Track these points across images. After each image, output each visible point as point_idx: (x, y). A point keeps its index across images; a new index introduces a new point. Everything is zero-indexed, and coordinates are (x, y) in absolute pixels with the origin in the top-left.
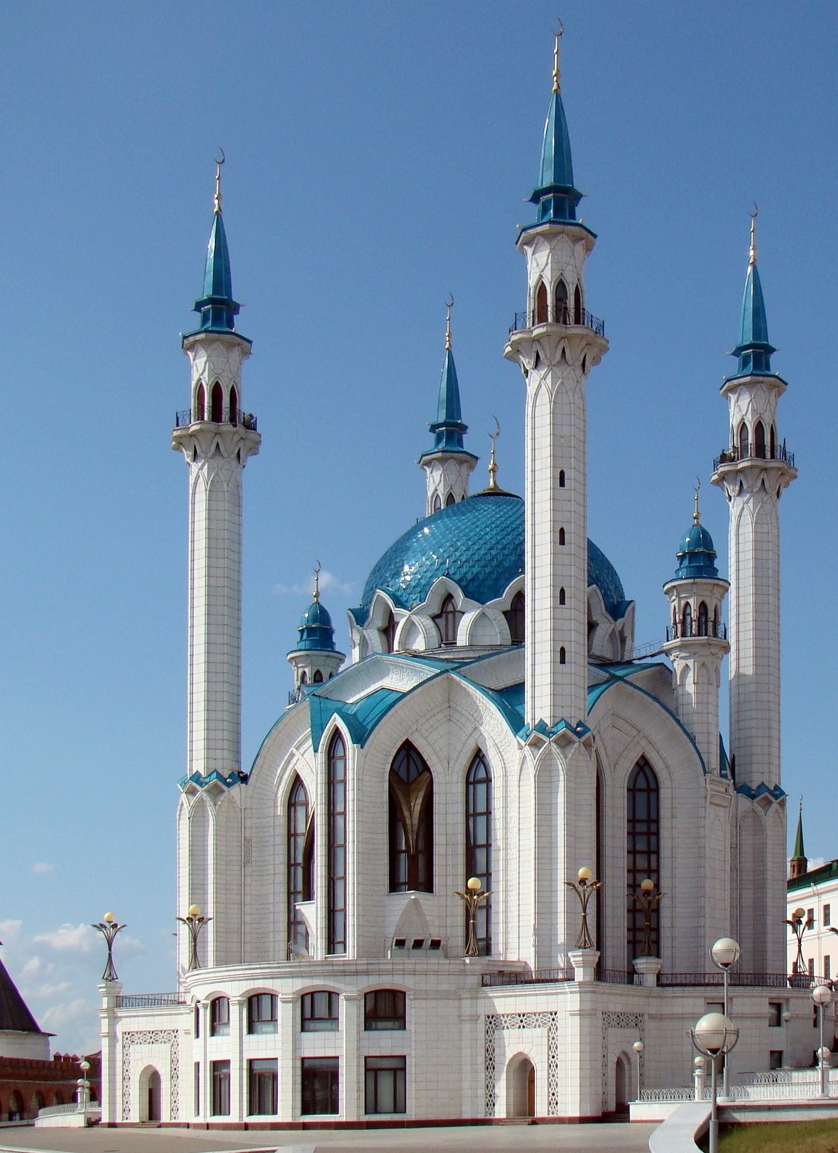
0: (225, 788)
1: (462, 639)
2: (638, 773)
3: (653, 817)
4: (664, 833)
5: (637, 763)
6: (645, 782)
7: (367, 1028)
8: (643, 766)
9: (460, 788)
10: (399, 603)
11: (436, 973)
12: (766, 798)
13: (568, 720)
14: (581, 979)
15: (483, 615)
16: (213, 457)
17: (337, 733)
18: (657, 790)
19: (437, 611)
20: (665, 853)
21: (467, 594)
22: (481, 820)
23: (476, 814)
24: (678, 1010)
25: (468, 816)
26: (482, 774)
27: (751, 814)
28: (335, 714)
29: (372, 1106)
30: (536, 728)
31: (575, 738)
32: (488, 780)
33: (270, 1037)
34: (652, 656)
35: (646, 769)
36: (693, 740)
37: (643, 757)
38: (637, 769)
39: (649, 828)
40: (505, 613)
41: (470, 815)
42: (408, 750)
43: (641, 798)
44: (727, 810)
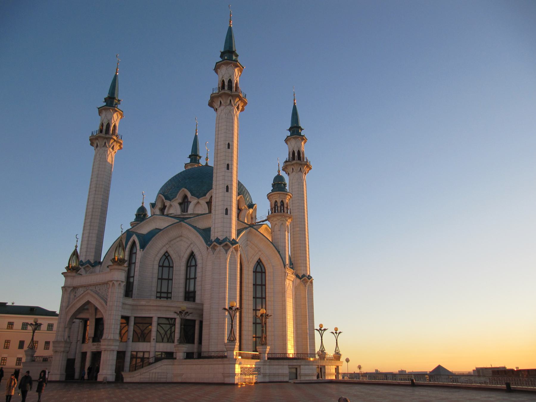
1: (190, 211)
3: (264, 283)
5: (257, 261)
6: (260, 269)
8: (259, 262)
9: (183, 268)
10: (167, 198)
12: (304, 279)
15: (198, 203)
16: (103, 146)
17: (134, 243)
18: (265, 273)
19: (180, 201)
21: (193, 194)
22: (192, 281)
23: (190, 279)
25: (186, 279)
26: (193, 263)
28: (134, 236)
30: (215, 241)
32: (196, 266)
34: (263, 221)
35: (261, 263)
36: (279, 252)
37: (259, 259)
40: (207, 203)
41: (187, 279)
43: (259, 275)
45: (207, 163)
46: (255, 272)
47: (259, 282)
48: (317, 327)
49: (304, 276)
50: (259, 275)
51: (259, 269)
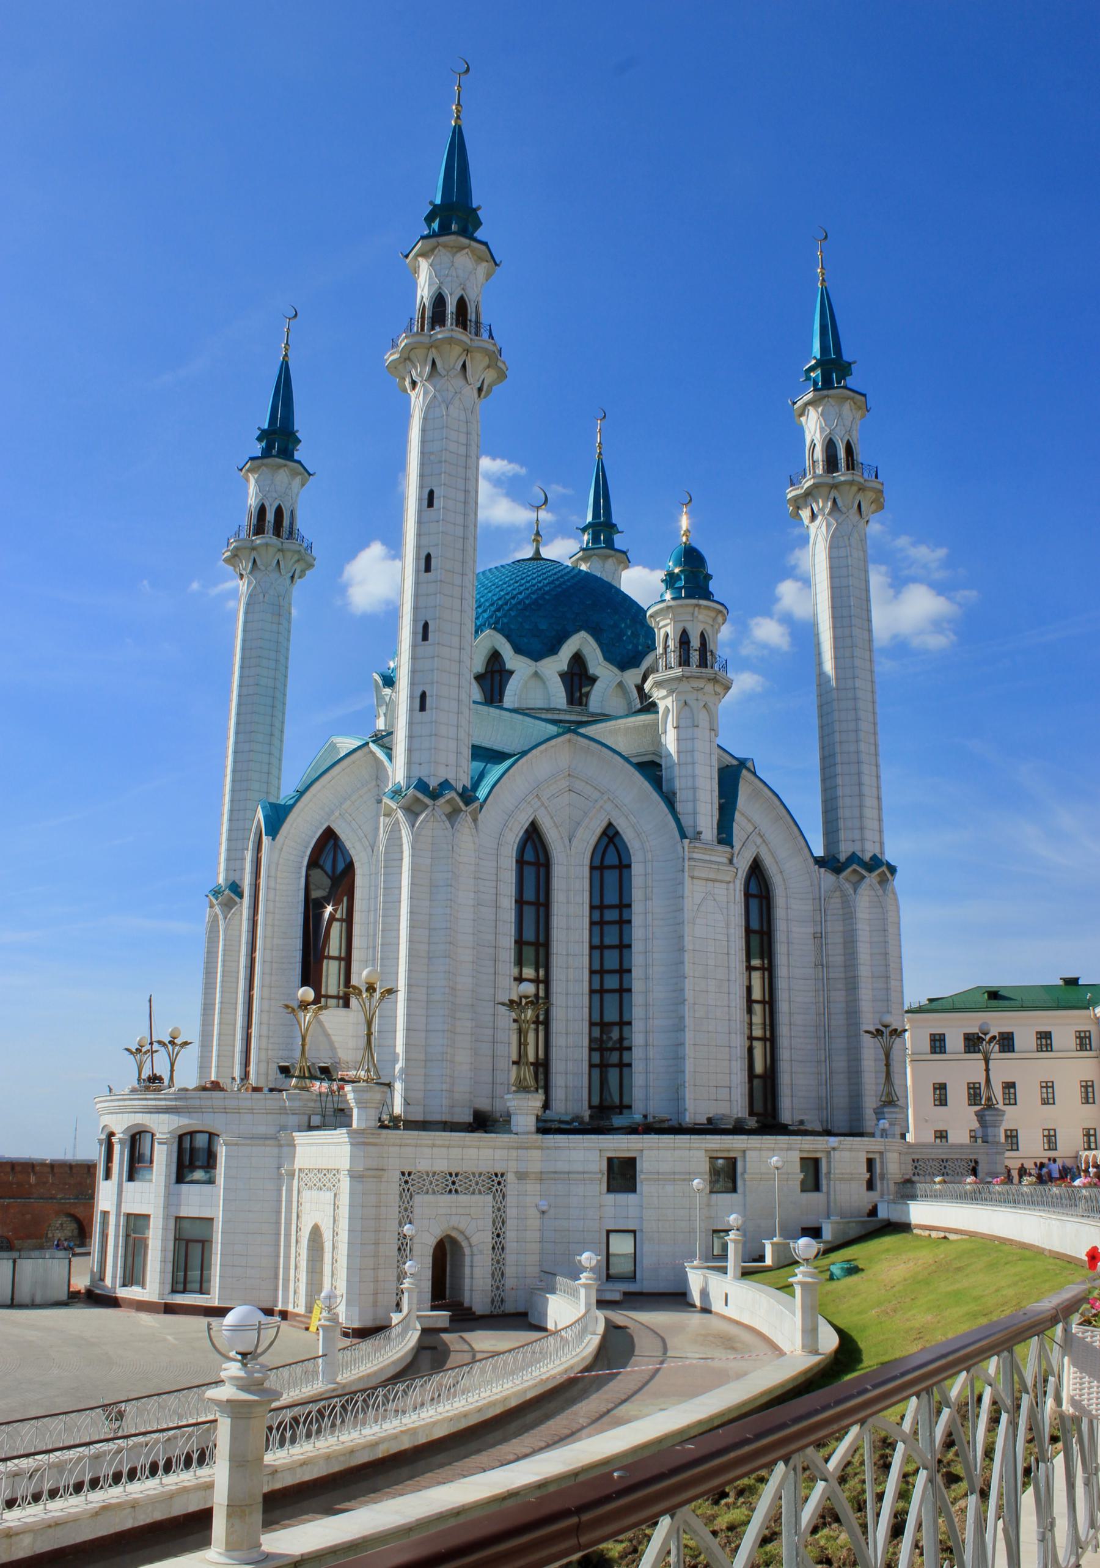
0: (237, 899)
2: (607, 847)
4: (637, 920)
5: (604, 833)
7: (180, 1179)
8: (610, 837)
11: (251, 1110)
13: (425, 779)
14: (363, 1126)
18: (629, 866)
20: (637, 947)
24: (561, 1166)
27: (838, 894)
29: (180, 1285)
31: (427, 800)
33: (146, 1185)
36: (670, 800)
37: (610, 825)
38: (605, 840)
39: (602, 916)
42: (329, 839)
43: (611, 877)
44: (731, 885)
45: (537, 552)
46: (598, 868)
47: (611, 898)
48: (869, 1022)
49: (853, 858)
50: (611, 877)
51: (611, 859)
